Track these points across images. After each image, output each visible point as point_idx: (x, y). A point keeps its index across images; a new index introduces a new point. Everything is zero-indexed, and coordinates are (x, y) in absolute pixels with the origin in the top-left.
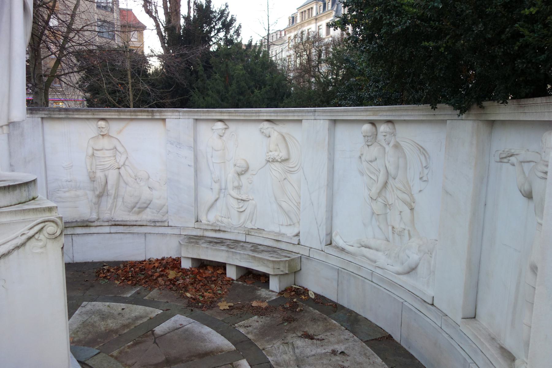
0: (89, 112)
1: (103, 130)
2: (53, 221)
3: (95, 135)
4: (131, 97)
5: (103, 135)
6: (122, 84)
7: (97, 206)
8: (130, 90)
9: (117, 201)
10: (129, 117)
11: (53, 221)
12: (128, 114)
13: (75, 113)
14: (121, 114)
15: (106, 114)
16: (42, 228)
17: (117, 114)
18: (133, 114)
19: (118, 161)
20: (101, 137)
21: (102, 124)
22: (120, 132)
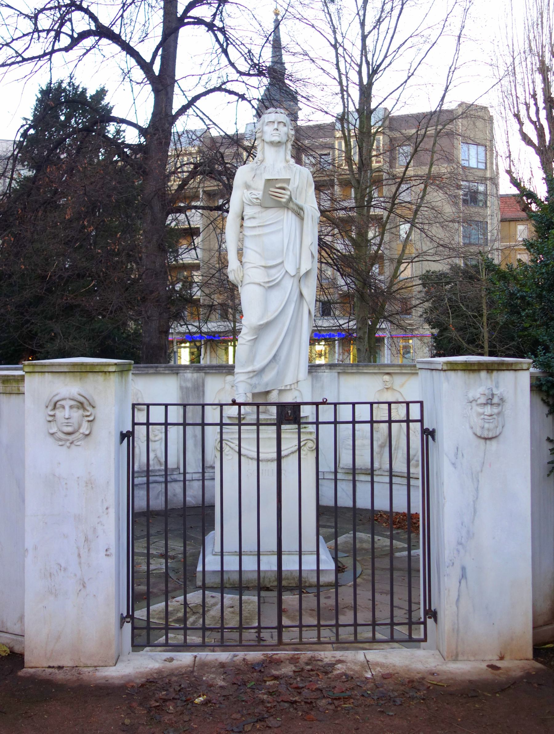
0: (375, 367)
1: (388, 384)
2: (311, 440)
3: (380, 388)
4: (486, 335)
5: (387, 389)
6: (475, 317)
7: (379, 455)
8: (485, 324)
9: (397, 453)
10: (410, 371)
11: (311, 440)
12: (409, 368)
13: (365, 368)
14: (403, 368)
15: (389, 368)
16: (306, 444)
17: (399, 368)
18: (413, 368)
19: (400, 413)
20: (385, 390)
21: (387, 377)
22: (402, 385)
